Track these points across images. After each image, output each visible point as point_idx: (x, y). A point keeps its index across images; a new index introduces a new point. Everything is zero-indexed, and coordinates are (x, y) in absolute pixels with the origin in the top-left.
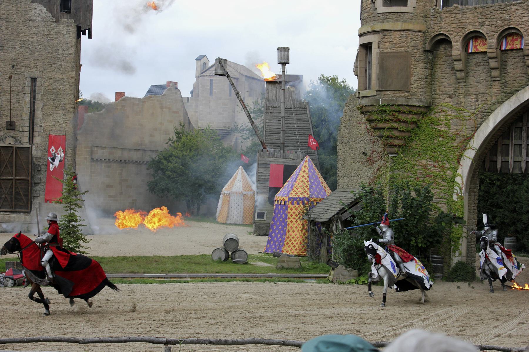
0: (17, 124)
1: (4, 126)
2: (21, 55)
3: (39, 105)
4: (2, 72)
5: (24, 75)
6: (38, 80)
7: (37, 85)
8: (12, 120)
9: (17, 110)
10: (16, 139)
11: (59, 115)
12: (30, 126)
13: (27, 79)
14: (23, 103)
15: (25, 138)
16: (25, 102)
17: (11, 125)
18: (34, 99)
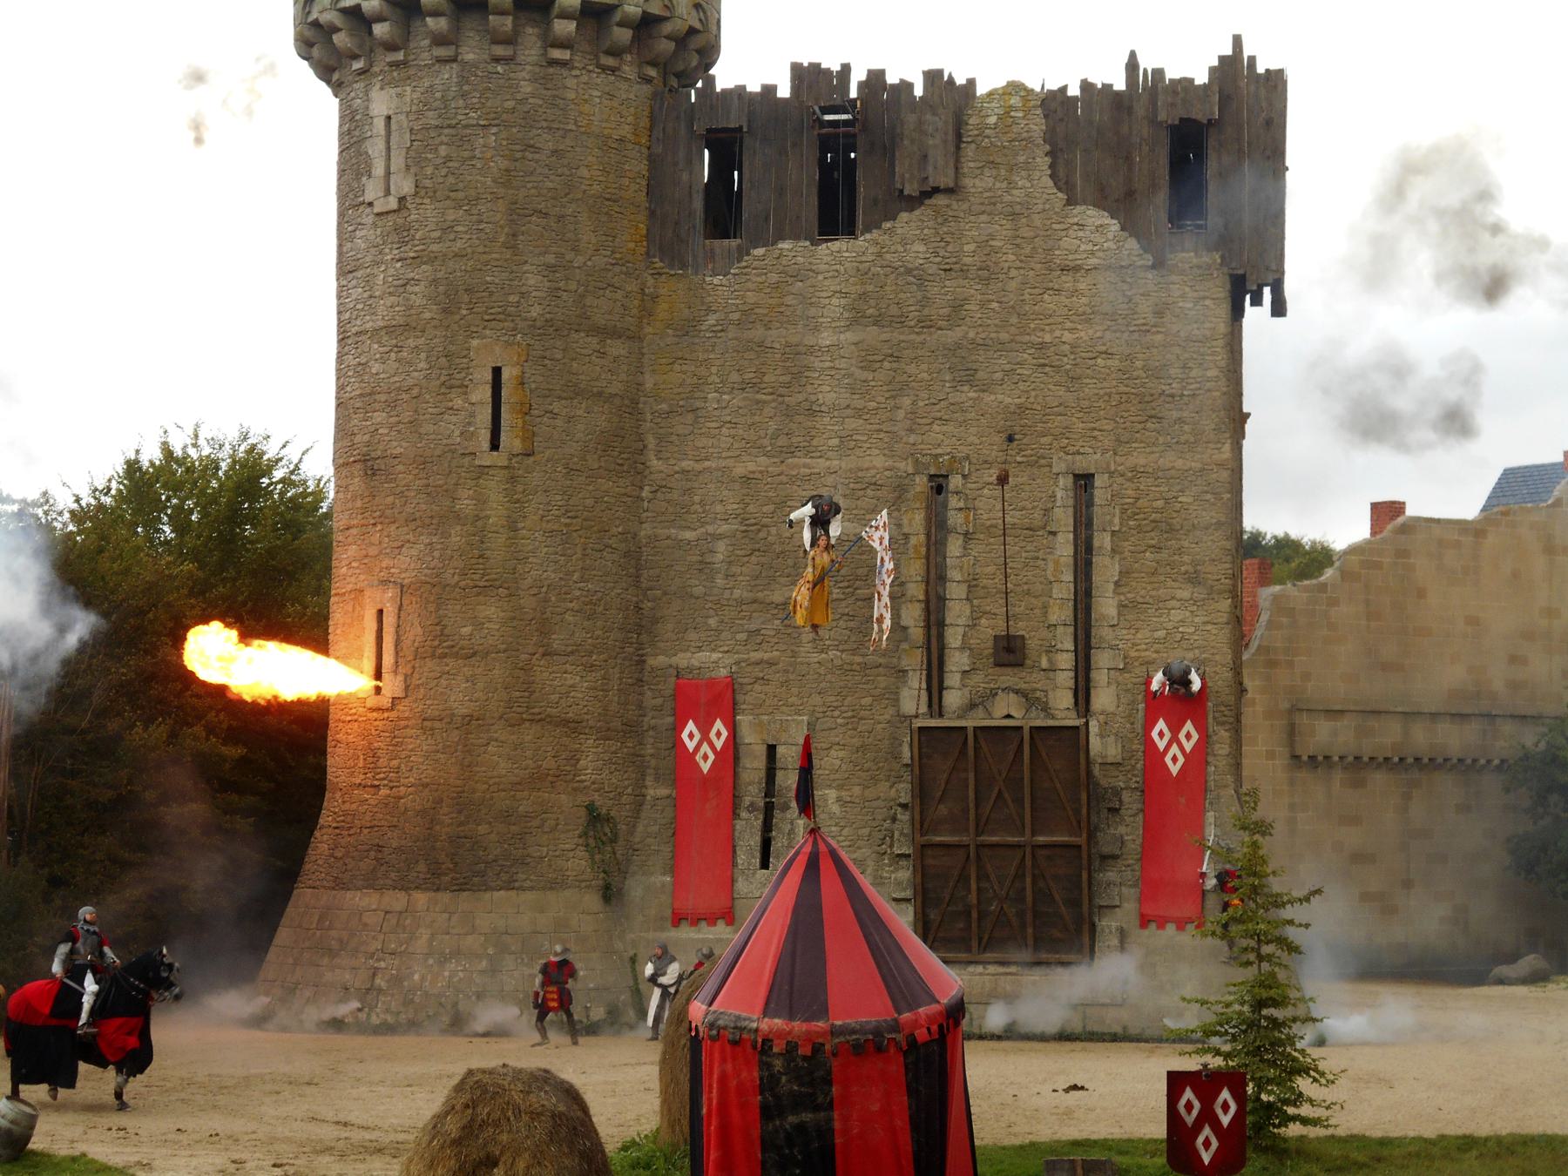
0: (1032, 644)
1: (986, 652)
2: (1036, 397)
3: (1106, 570)
4: (974, 461)
5: (1051, 466)
6: (1098, 482)
7: (1097, 501)
8: (1012, 632)
9: (1028, 593)
10: (1029, 699)
11: (1178, 604)
12: (1076, 651)
13: (1062, 481)
14: (1051, 567)
15: (1059, 693)
16: (1057, 563)
17: (1009, 650)
18: (1089, 549)
